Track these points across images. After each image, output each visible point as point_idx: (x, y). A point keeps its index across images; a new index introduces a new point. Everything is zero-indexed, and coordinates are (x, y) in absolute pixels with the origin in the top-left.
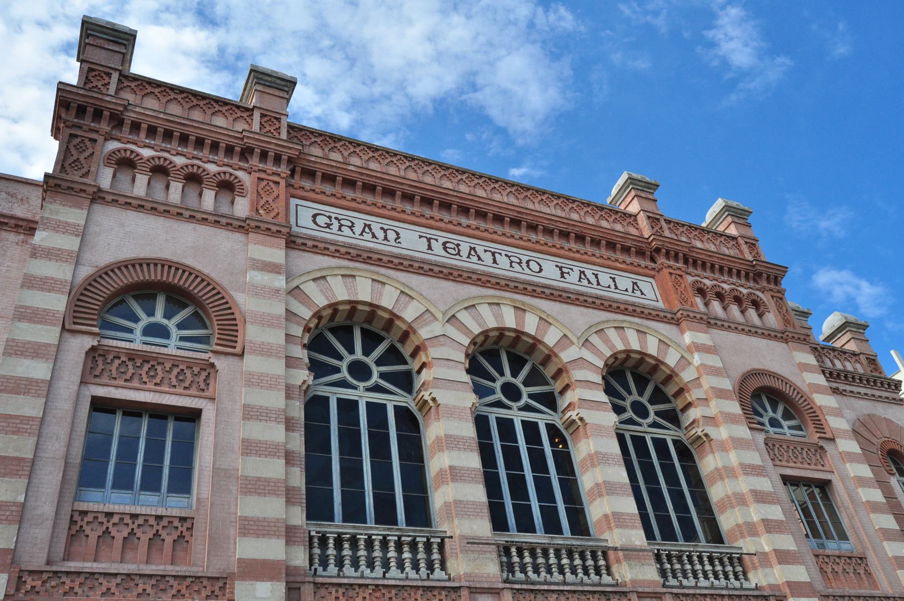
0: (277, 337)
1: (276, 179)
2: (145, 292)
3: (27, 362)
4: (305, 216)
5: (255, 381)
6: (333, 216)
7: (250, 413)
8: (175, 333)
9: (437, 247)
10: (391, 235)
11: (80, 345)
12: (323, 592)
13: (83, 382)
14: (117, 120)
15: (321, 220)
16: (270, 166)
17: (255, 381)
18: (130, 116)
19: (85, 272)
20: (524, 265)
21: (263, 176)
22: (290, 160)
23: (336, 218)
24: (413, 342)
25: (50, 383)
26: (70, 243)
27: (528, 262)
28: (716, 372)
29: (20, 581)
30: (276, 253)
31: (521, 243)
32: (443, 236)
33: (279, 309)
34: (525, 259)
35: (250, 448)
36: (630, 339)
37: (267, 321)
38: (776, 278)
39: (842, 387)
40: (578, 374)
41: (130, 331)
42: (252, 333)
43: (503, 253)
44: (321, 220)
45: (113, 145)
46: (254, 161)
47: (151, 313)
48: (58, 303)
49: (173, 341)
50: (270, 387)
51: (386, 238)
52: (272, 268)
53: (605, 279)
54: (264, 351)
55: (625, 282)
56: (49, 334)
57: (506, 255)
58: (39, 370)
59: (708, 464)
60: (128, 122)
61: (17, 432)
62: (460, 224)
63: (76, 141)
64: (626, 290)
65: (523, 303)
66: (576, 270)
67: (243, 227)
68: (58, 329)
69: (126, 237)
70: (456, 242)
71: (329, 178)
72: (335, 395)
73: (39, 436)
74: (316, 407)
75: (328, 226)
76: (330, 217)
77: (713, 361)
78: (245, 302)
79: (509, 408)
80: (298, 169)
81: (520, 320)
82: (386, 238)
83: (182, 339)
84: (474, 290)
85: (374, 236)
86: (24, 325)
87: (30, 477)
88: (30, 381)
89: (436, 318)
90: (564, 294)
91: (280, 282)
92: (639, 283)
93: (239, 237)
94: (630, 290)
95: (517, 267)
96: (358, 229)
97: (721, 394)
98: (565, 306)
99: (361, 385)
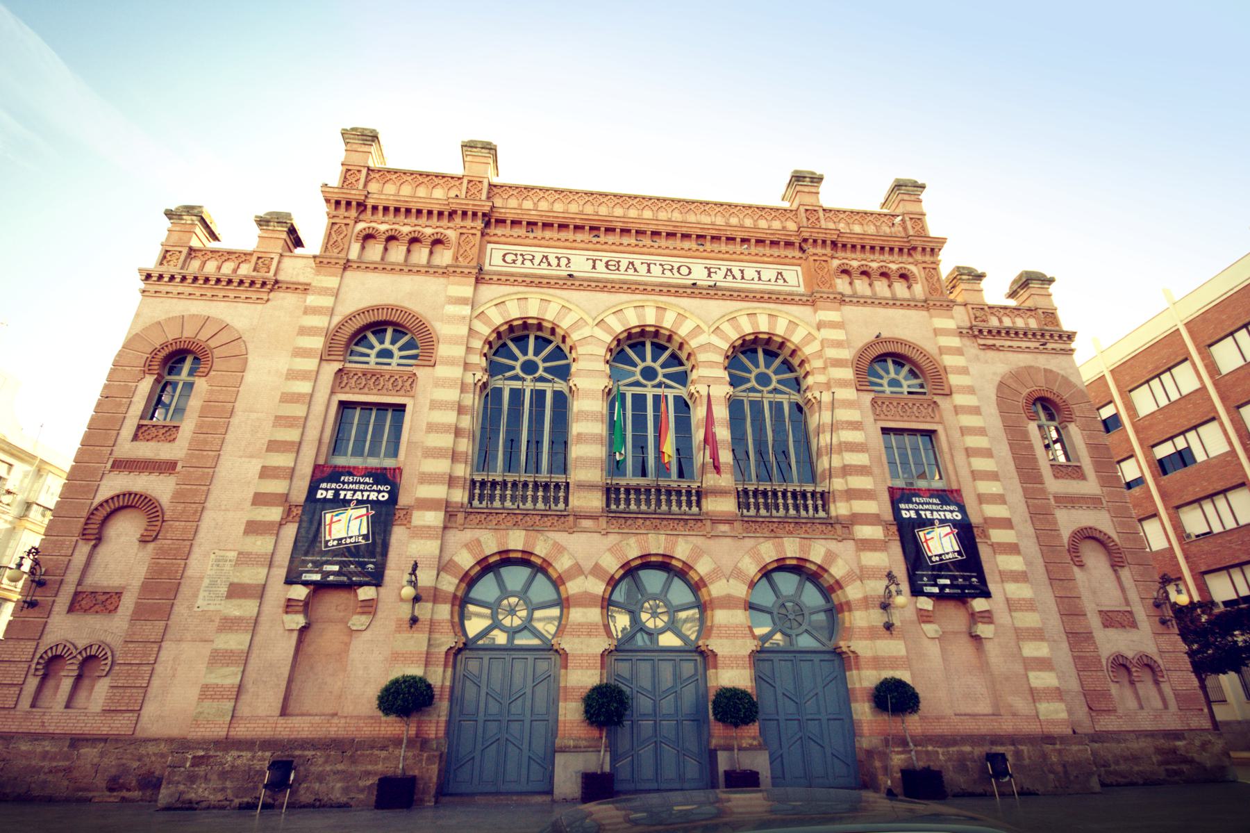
0: (459, 351)
1: (473, 231)
2: (378, 328)
3: (298, 383)
5: (440, 383)
7: (435, 405)
8: (397, 353)
9: (600, 266)
10: (564, 262)
11: (331, 368)
12: (472, 517)
13: (333, 392)
14: (361, 206)
15: (509, 258)
16: (469, 223)
17: (440, 383)
18: (370, 202)
19: (336, 320)
20: (675, 271)
22: (484, 215)
24: (569, 342)
25: (311, 395)
26: (328, 301)
28: (839, 344)
29: (290, 511)
30: (465, 289)
31: (675, 252)
32: (606, 256)
33: (464, 331)
34: (676, 265)
35: (432, 428)
36: (761, 321)
37: (453, 341)
38: (932, 250)
39: (998, 343)
40: (702, 357)
41: (368, 355)
42: (443, 350)
44: (509, 258)
45: (361, 226)
46: (458, 220)
47: (382, 342)
48: (318, 343)
49: (395, 361)
50: (451, 387)
51: (559, 265)
52: (462, 301)
53: (750, 273)
54: (451, 362)
55: (769, 273)
56: (311, 364)
58: (304, 387)
59: (813, 421)
60: (369, 207)
61: (291, 426)
63: (336, 227)
65: (665, 303)
66: (724, 269)
67: (445, 272)
68: (317, 360)
69: (367, 291)
71: (515, 223)
72: (507, 386)
73: (304, 427)
74: (491, 397)
75: (514, 262)
77: (838, 335)
78: (442, 329)
79: (645, 386)
81: (660, 317)
82: (559, 265)
83: (401, 357)
85: (549, 264)
86: (298, 360)
87: (298, 452)
88: (299, 394)
89: (587, 324)
91: (466, 310)
92: (784, 273)
94: (773, 279)
95: (668, 273)
96: (537, 261)
97: (838, 363)
98: (704, 301)
99: (529, 377)
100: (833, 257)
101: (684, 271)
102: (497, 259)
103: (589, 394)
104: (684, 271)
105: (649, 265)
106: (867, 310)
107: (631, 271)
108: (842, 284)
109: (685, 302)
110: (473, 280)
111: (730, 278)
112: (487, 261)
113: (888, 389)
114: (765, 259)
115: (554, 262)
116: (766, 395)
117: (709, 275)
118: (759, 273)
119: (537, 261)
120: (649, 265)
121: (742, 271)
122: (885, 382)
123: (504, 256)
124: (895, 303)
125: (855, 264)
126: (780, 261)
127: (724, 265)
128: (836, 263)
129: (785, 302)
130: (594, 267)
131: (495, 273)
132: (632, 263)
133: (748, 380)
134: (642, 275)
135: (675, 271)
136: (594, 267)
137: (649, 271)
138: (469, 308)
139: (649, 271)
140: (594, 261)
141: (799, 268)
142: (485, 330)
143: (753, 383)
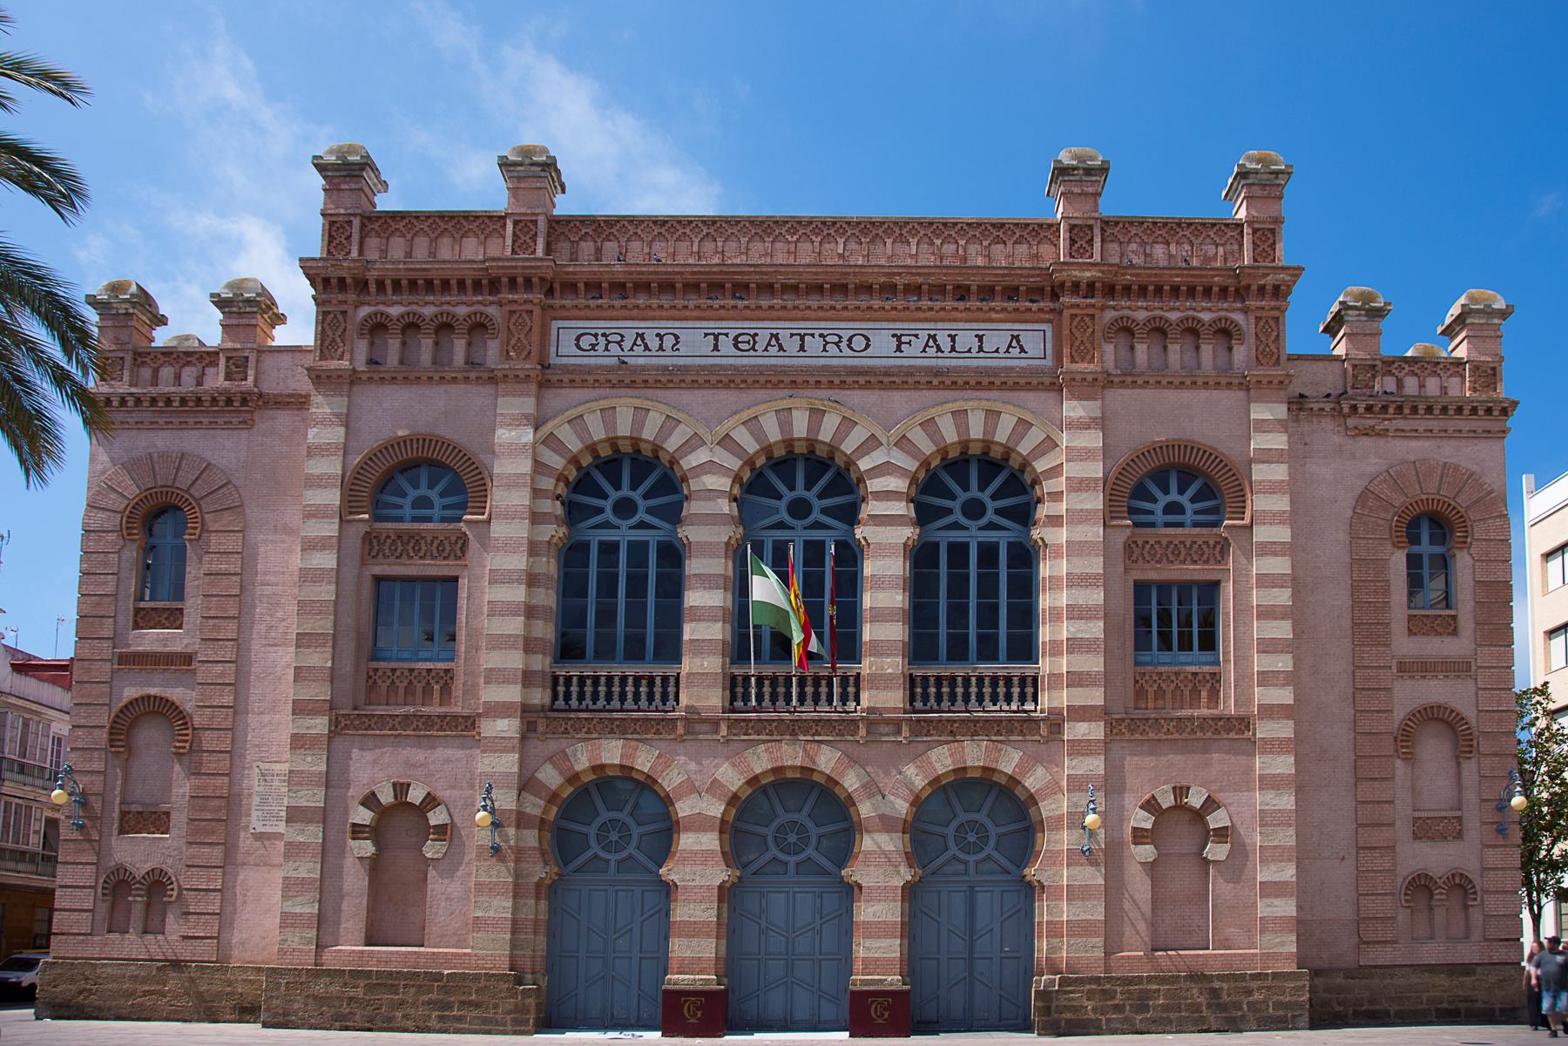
1: (529, 307)
4: (568, 342)
6: (600, 332)
9: (726, 345)
15: (586, 342)
21: (515, 307)
23: (603, 335)
27: (850, 340)
32: (734, 327)
34: (846, 335)
43: (817, 333)
44: (586, 342)
49: (436, 512)
51: (661, 348)
53: (966, 340)
55: (997, 339)
57: (821, 335)
62: (760, 307)
64: (997, 351)
66: (924, 335)
70: (752, 332)
75: (593, 347)
76: (596, 335)
80: (557, 286)
82: (661, 348)
83: (445, 507)
84: (761, 394)
85: (647, 348)
90: (886, 380)
93: (489, 389)
98: (884, 394)
100: (1103, 308)
101: (859, 343)
102: (568, 347)
103: (707, 550)
104: (859, 343)
105: (802, 338)
106: (1148, 395)
107: (773, 350)
108: (1109, 355)
109: (856, 397)
110: (534, 387)
111: (932, 351)
112: (553, 349)
113: (1159, 517)
114: (994, 315)
115: (654, 343)
116: (974, 532)
117: (899, 349)
118: (980, 338)
119: (627, 344)
120: (802, 338)
121: (953, 338)
122: (1158, 508)
123: (578, 339)
124: (1191, 381)
125: (1141, 315)
126: (1019, 316)
127: (924, 330)
128: (1110, 315)
129: (1016, 387)
130: (716, 348)
131: (567, 369)
132: (776, 336)
133: (950, 511)
134: (792, 358)
135: (844, 345)
136: (716, 348)
137: (802, 348)
138: (531, 431)
139: (802, 348)
140: (716, 337)
141: (1047, 327)
142: (557, 462)
143: (958, 516)
